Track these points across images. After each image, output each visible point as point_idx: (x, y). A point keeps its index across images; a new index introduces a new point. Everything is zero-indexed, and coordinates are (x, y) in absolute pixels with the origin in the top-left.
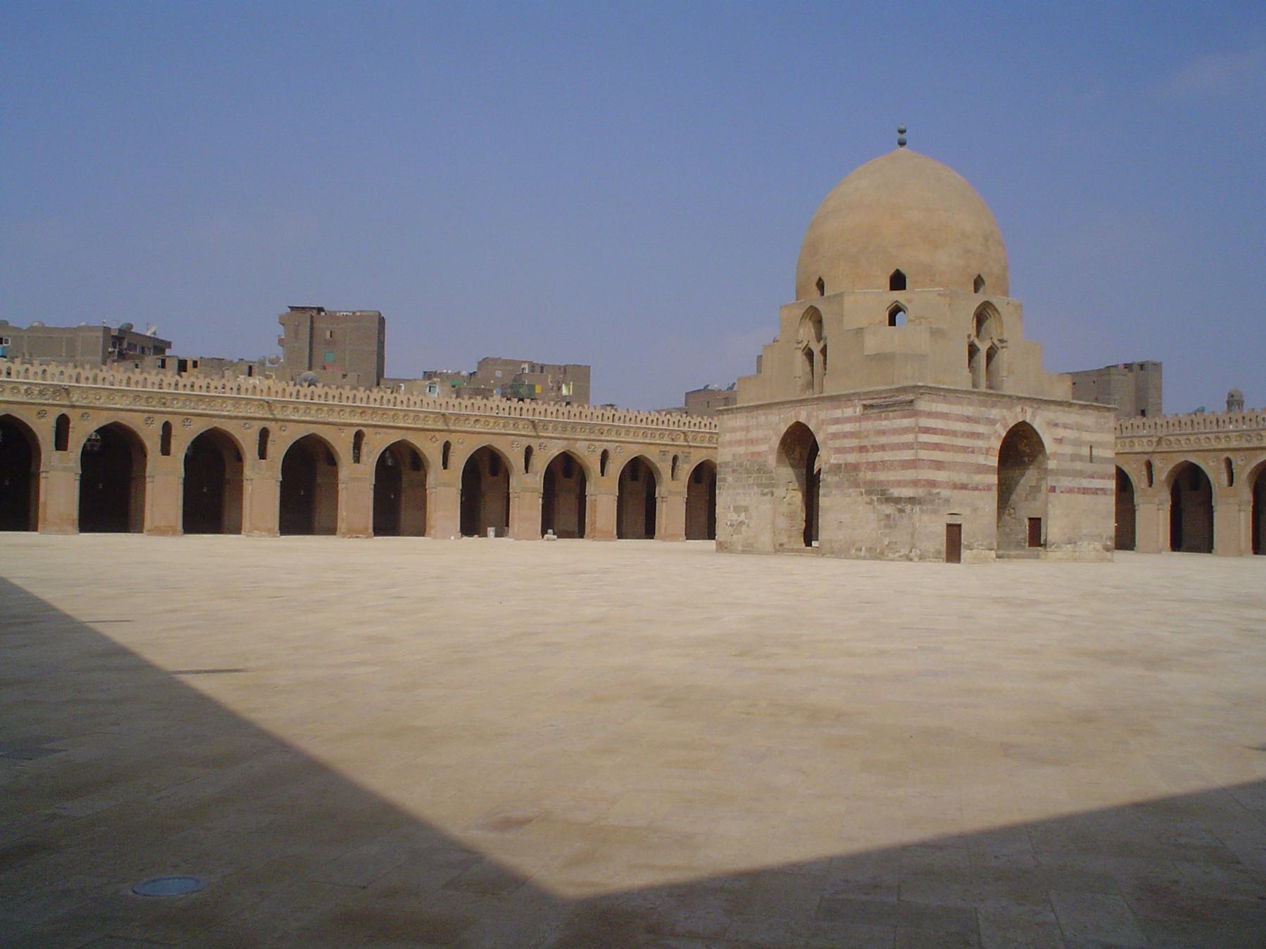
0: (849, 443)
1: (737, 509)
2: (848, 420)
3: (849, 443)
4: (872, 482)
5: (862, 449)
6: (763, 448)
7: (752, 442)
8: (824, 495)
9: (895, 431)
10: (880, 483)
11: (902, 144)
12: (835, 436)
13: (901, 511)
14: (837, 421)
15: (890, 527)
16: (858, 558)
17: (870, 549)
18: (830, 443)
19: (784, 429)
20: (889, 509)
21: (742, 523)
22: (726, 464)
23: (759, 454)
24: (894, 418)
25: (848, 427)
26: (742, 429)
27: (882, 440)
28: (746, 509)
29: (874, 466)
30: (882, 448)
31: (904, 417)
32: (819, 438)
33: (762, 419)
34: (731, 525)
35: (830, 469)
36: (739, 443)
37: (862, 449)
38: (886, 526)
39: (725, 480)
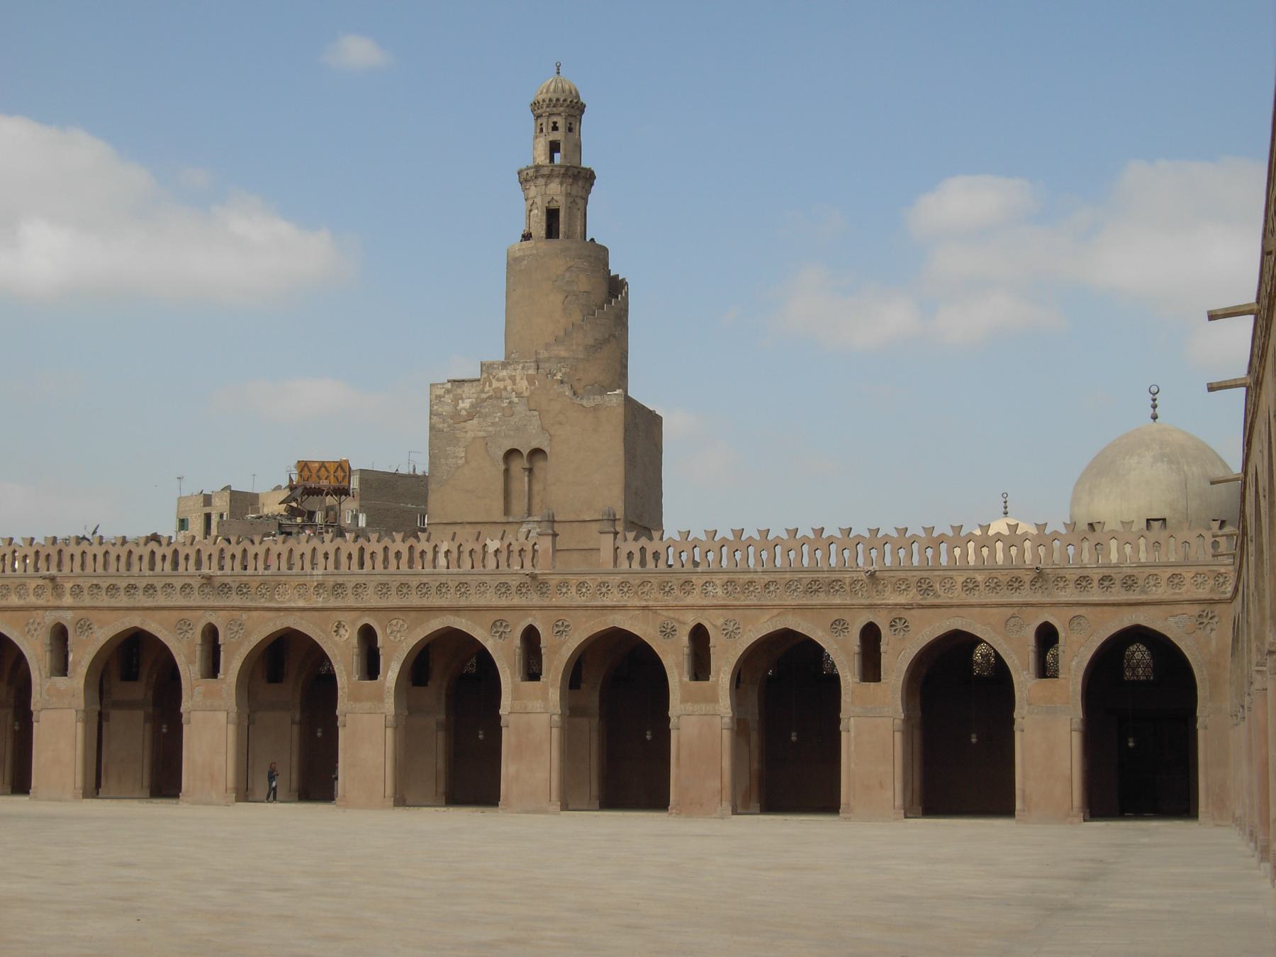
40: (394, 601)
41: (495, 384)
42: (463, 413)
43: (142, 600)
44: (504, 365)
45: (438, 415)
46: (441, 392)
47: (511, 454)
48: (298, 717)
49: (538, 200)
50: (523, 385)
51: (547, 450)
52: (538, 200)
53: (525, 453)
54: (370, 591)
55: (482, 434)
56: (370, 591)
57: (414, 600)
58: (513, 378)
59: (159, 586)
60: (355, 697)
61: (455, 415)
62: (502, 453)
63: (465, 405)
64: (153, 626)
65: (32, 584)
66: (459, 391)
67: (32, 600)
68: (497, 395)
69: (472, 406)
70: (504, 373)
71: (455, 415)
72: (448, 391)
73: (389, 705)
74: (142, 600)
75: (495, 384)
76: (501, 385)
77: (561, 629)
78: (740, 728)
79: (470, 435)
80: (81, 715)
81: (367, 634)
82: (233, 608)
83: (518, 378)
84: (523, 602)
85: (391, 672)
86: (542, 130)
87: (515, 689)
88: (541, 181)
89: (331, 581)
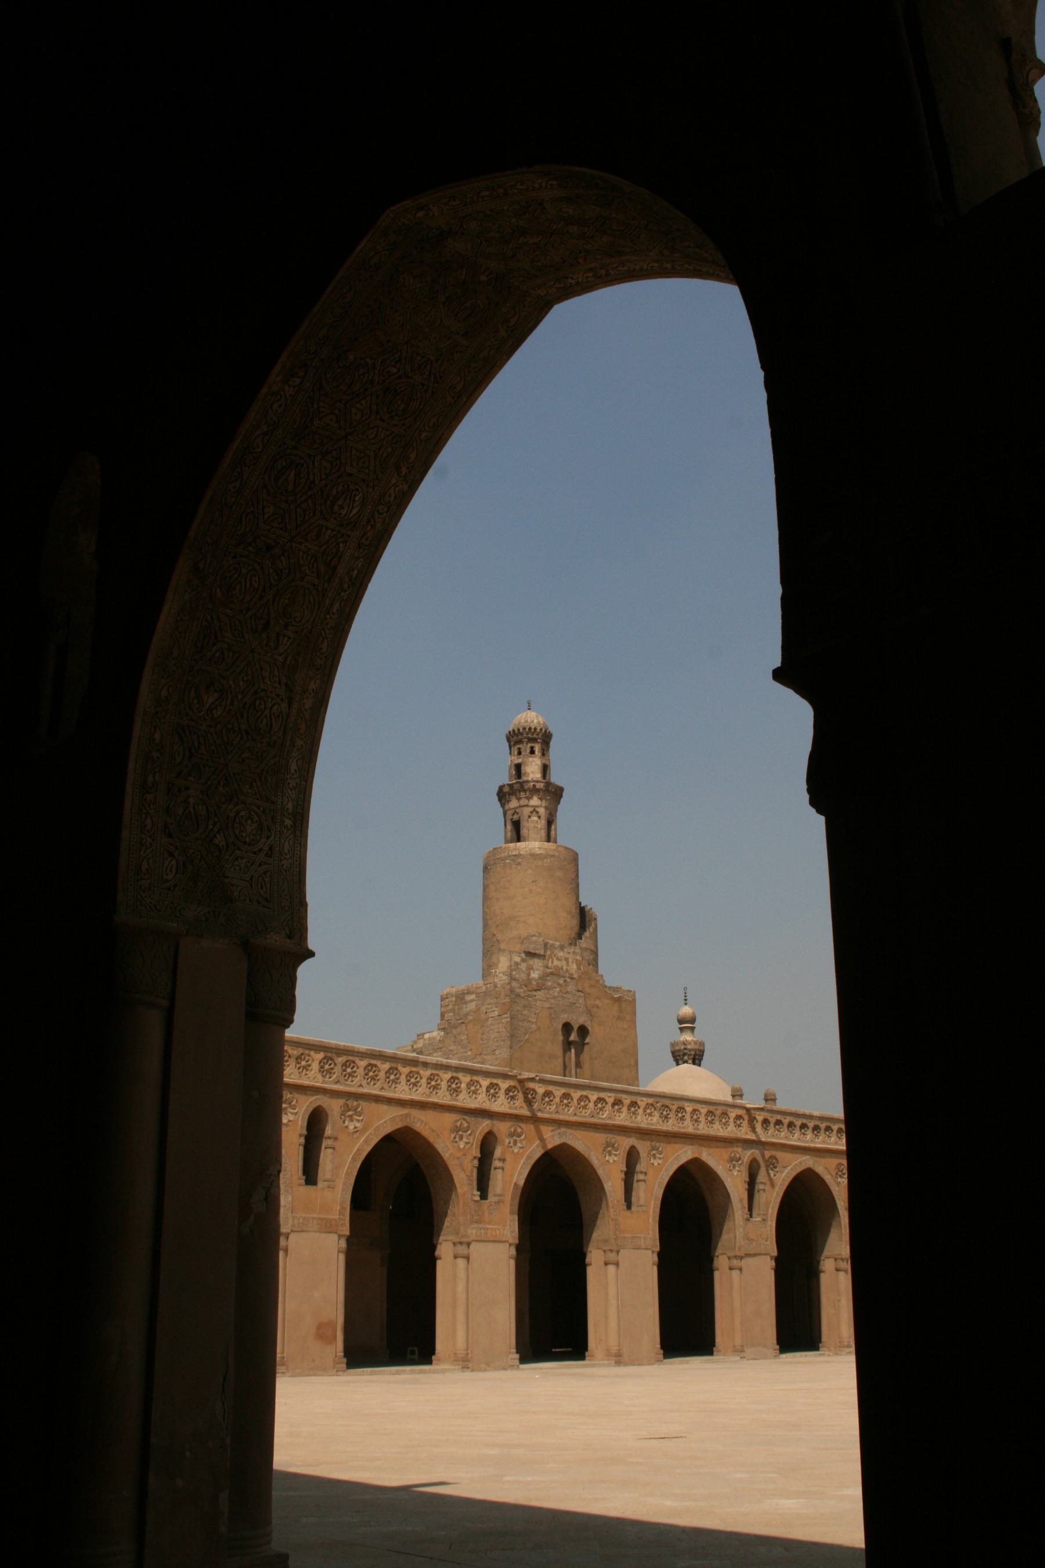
41: (556, 963)
42: (534, 983)
44: (562, 948)
45: (515, 980)
46: (517, 959)
47: (567, 1027)
51: (589, 1028)
52: (542, 811)
53: (576, 1027)
55: (547, 1005)
58: (567, 959)
61: (528, 982)
62: (560, 1027)
63: (535, 975)
66: (531, 962)
67: (729, 1131)
68: (556, 973)
69: (540, 978)
70: (561, 954)
71: (528, 982)
72: (523, 961)
74: (809, 1140)
75: (556, 963)
83: (570, 960)
86: (532, 752)
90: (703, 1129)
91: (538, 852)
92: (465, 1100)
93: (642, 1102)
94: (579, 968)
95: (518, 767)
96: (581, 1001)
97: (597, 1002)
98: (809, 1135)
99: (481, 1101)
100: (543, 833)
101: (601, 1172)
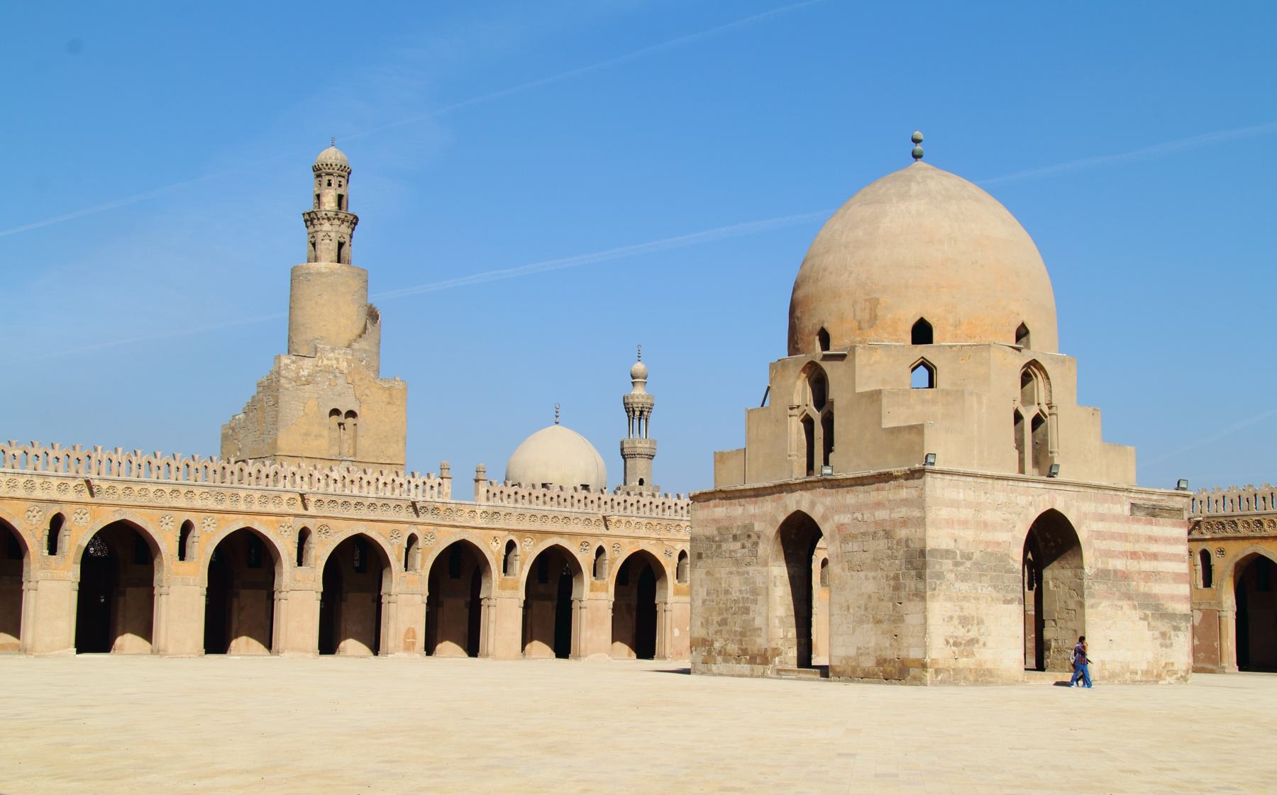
0: (1118, 546)
1: (964, 621)
2: (1116, 518)
3: (1118, 546)
4: (1147, 596)
5: (1134, 555)
6: (1002, 536)
7: (986, 524)
8: (1092, 607)
9: (1167, 540)
10: (1155, 597)
11: (916, 156)
12: (1100, 535)
13: (1176, 628)
14: (1102, 518)
15: (1166, 646)
16: (1134, 682)
17: (1146, 673)
18: (1098, 544)
19: (1034, 515)
20: (1164, 626)
21: (972, 642)
22: (947, 553)
23: (998, 544)
24: (1164, 525)
25: (1117, 528)
26: (968, 505)
27: (1154, 548)
28: (981, 622)
29: (1149, 576)
30: (1155, 556)
31: (1174, 525)
32: (1082, 535)
33: (1001, 497)
34: (955, 644)
35: (1097, 575)
36: (965, 524)
37: (1134, 555)
38: (1162, 645)
39: (940, 576)
40: (526, 525)
41: (325, 362)
43: (364, 513)
44: (333, 350)
48: (634, 603)
49: (333, 235)
50: (344, 365)
53: (344, 413)
54: (514, 518)
56: (514, 518)
57: (537, 526)
58: (337, 359)
59: (379, 504)
60: (503, 586)
64: (373, 532)
65: (286, 497)
67: (284, 508)
68: (327, 370)
71: (298, 378)
72: (293, 362)
73: (521, 594)
74: (364, 513)
76: (329, 363)
77: (617, 547)
78: (616, 608)
79: (307, 395)
80: (320, 597)
81: (511, 546)
82: (430, 524)
84: (597, 532)
85: (522, 571)
86: (329, 184)
87: (592, 584)
88: (337, 222)
89: (491, 510)
90: (256, 507)
91: (324, 270)
92: (38, 494)
93: (197, 491)
94: (349, 366)
95: (318, 196)
96: (351, 391)
97: (367, 391)
98: (365, 510)
99: (55, 495)
100: (334, 255)
101: (156, 537)
